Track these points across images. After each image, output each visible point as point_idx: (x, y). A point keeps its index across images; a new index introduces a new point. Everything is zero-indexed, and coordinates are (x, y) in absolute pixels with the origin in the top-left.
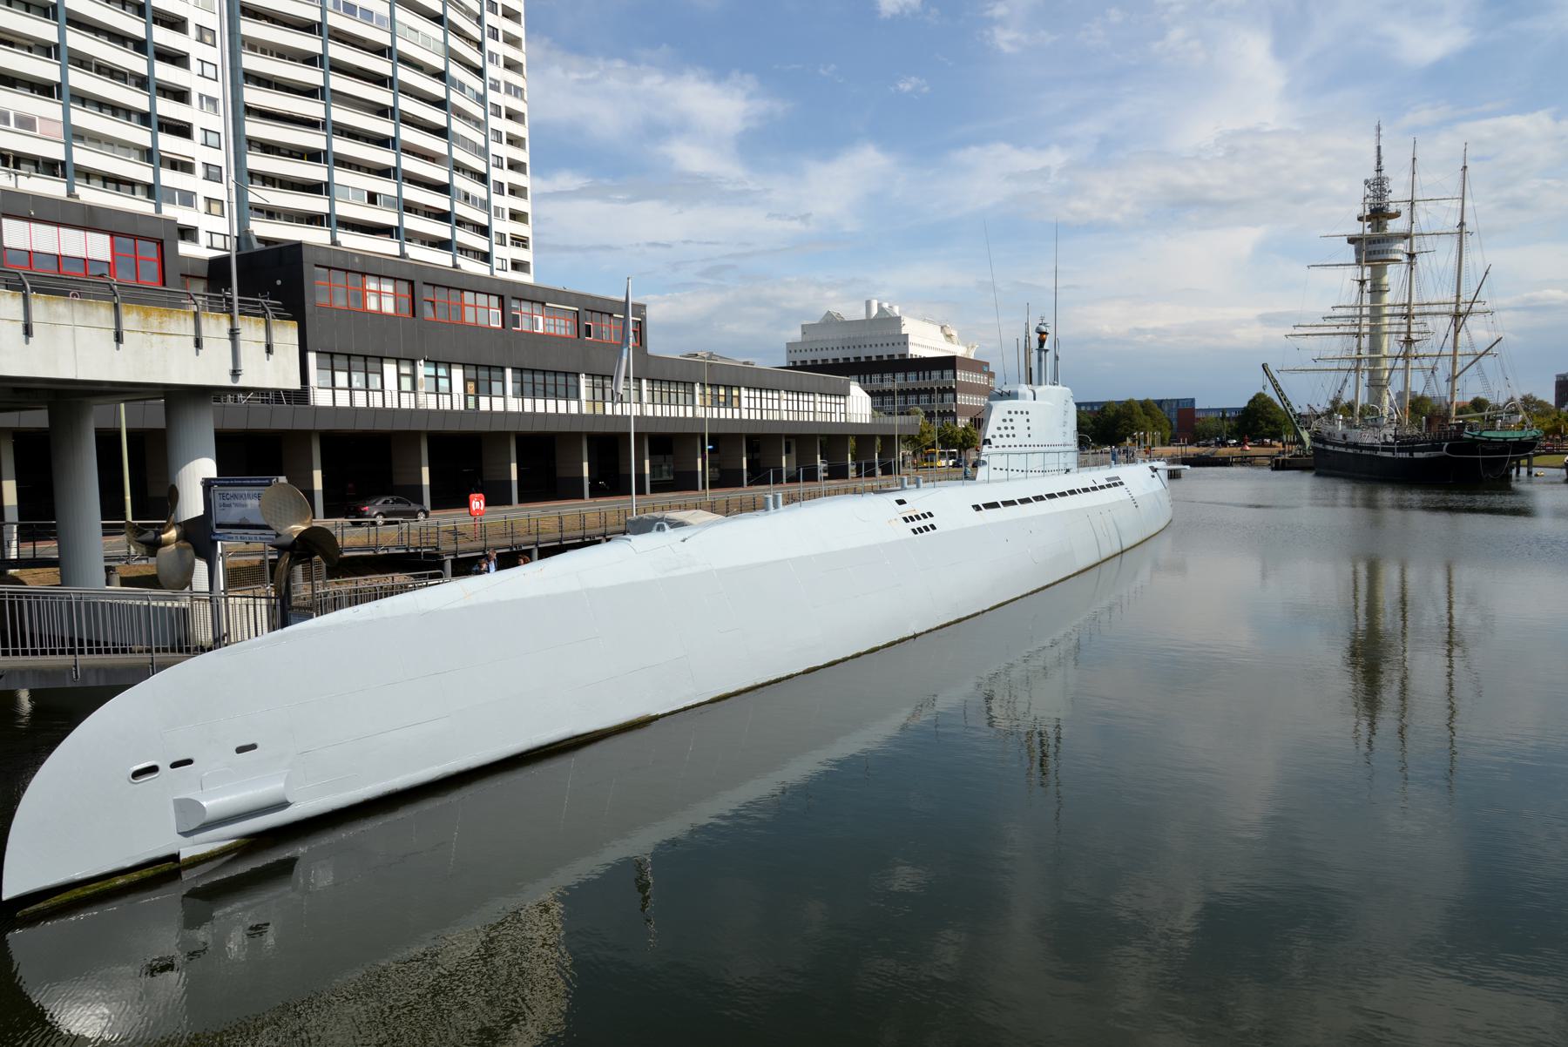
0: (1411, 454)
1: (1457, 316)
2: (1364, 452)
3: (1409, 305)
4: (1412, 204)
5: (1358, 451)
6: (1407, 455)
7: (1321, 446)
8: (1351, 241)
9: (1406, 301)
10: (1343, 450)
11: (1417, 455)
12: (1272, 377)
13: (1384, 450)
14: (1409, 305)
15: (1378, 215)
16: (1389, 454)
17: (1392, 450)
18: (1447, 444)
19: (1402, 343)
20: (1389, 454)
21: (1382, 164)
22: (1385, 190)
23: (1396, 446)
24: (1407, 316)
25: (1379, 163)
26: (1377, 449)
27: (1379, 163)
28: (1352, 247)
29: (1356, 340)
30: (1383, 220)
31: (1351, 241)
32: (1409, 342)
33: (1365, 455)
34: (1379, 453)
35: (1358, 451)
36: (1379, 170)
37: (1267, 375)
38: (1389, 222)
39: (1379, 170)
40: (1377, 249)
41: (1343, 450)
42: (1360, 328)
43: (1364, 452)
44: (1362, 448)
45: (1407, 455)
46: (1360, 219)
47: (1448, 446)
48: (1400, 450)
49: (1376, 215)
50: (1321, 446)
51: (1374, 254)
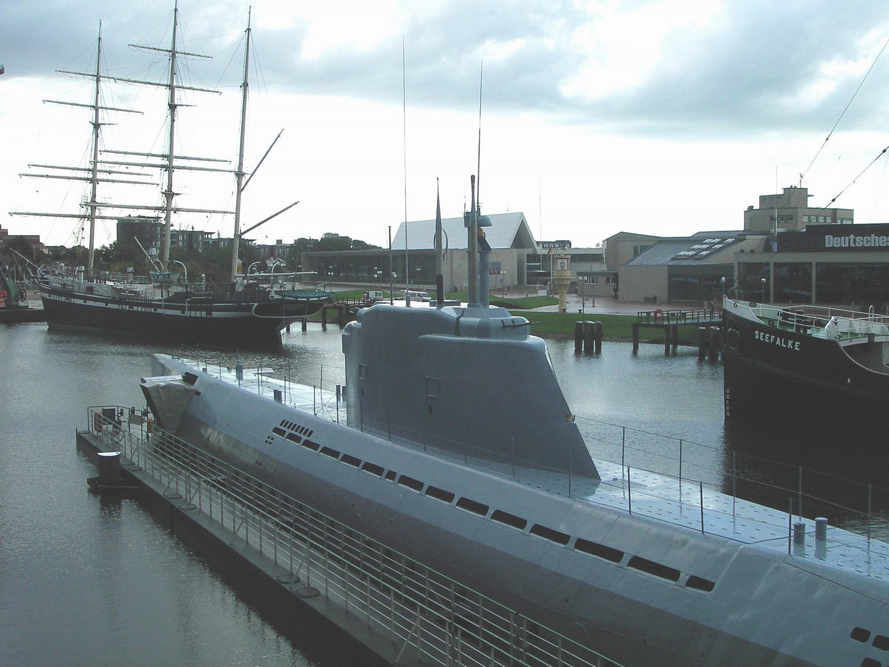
0: (209, 313)
1: (239, 174)
2: (135, 308)
3: (169, 157)
4: (174, 56)
5: (127, 308)
6: (204, 314)
7: (63, 299)
10: (103, 305)
11: (215, 314)
13: (166, 307)
16: (178, 313)
17: (183, 309)
18: (256, 304)
20: (178, 313)
23: (187, 305)
24: (169, 168)
26: (160, 306)
32: (169, 194)
33: (137, 312)
34: (159, 311)
35: (127, 308)
41: (103, 305)
43: (135, 308)
44: (131, 305)
45: (204, 314)
47: (257, 306)
48: (190, 309)
50: (63, 299)
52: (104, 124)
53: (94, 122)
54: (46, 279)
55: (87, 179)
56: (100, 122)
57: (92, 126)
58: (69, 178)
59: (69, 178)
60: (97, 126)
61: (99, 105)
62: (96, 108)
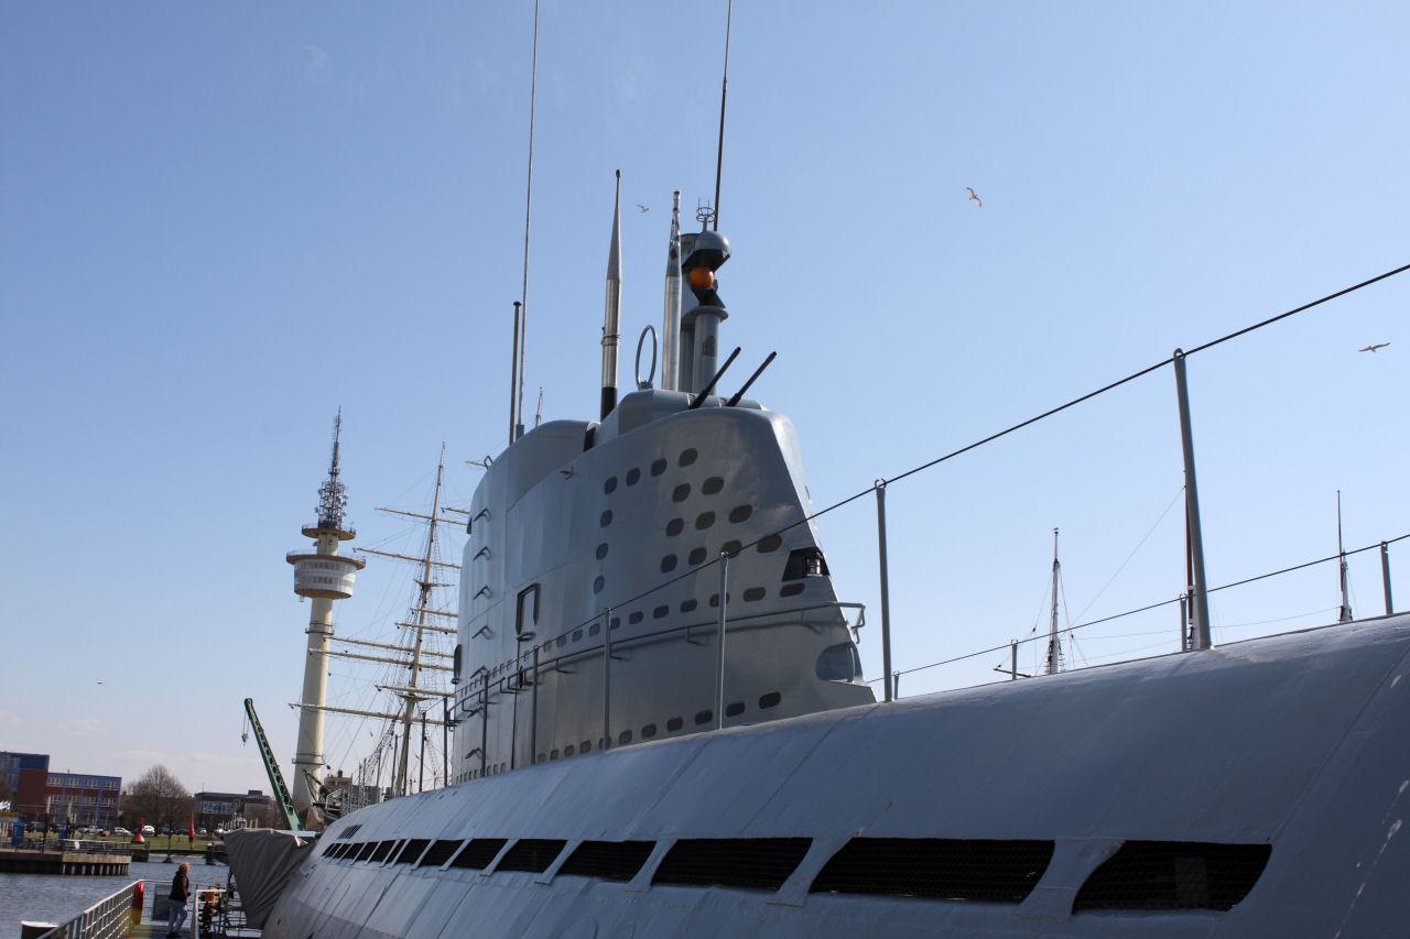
8: (291, 559)
9: (413, 646)
12: (258, 723)
14: (415, 651)
15: (328, 529)
19: (403, 700)
21: (338, 467)
22: (338, 500)
25: (334, 464)
27: (334, 464)
28: (291, 568)
29: (408, 673)
30: (335, 539)
31: (291, 559)
36: (334, 474)
37: (251, 718)
38: (340, 542)
39: (334, 474)
40: (323, 575)
42: (416, 656)
46: (306, 532)
49: (324, 530)
51: (320, 582)
52: (436, 585)
53: (423, 580)
54: (337, 808)
55: (405, 663)
56: (430, 581)
57: (418, 587)
58: (379, 660)
59: (379, 660)
60: (426, 587)
61: (432, 560)
62: (426, 562)
